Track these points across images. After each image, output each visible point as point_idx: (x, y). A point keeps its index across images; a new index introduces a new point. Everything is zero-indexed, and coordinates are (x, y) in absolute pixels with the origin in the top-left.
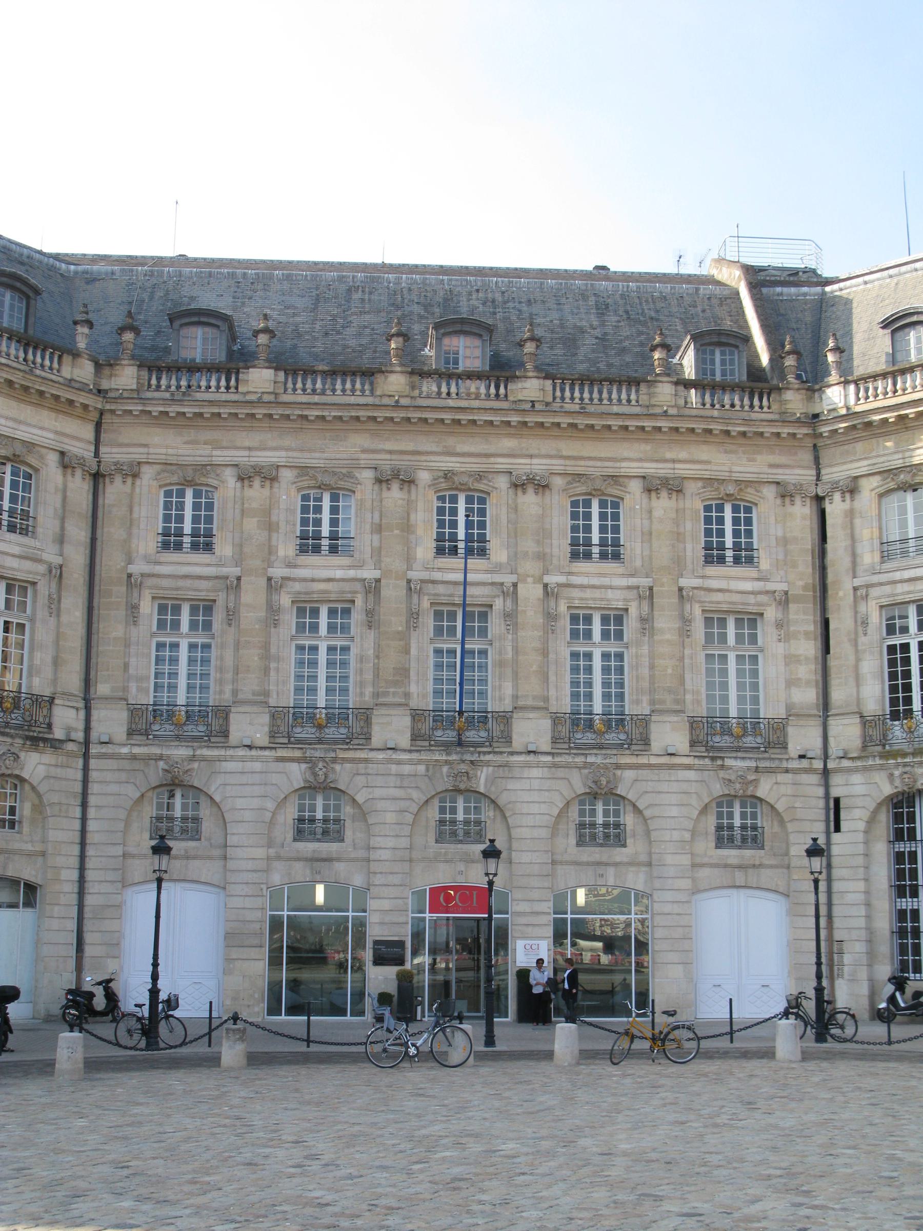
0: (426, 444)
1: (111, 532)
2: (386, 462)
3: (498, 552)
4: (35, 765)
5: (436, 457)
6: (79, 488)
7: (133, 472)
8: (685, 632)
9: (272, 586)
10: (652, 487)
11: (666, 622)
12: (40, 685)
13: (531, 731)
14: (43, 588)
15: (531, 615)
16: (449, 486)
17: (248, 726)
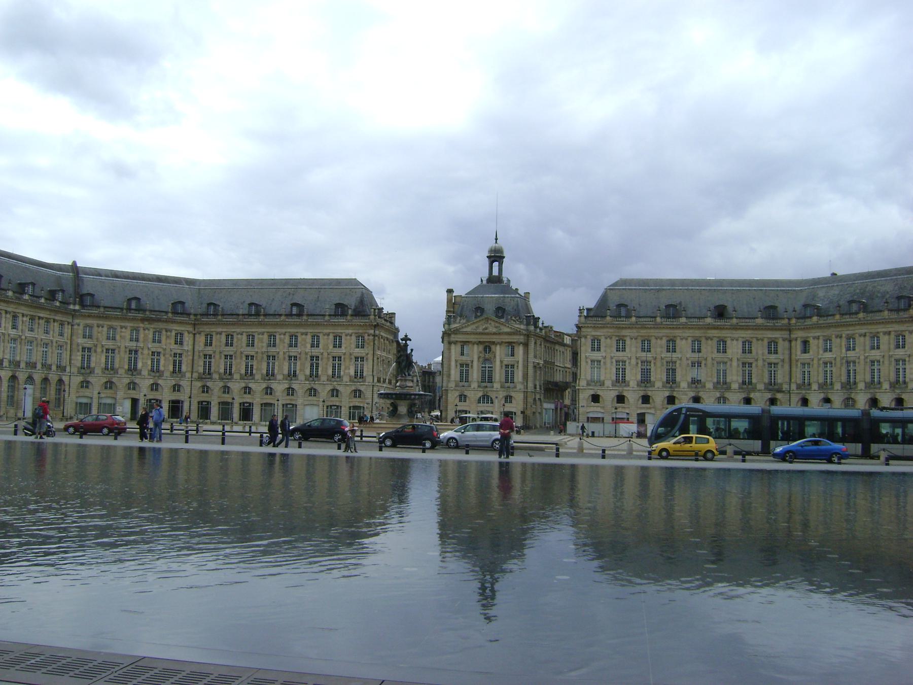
0: (844, 329)
1: (793, 351)
2: (837, 333)
3: (857, 350)
4: (779, 396)
5: (845, 332)
6: (787, 344)
7: (796, 340)
8: (890, 364)
9: (819, 359)
10: (885, 333)
11: (886, 362)
12: (779, 381)
13: (861, 386)
14: (780, 364)
15: (862, 362)
16: (849, 338)
17: (815, 386)
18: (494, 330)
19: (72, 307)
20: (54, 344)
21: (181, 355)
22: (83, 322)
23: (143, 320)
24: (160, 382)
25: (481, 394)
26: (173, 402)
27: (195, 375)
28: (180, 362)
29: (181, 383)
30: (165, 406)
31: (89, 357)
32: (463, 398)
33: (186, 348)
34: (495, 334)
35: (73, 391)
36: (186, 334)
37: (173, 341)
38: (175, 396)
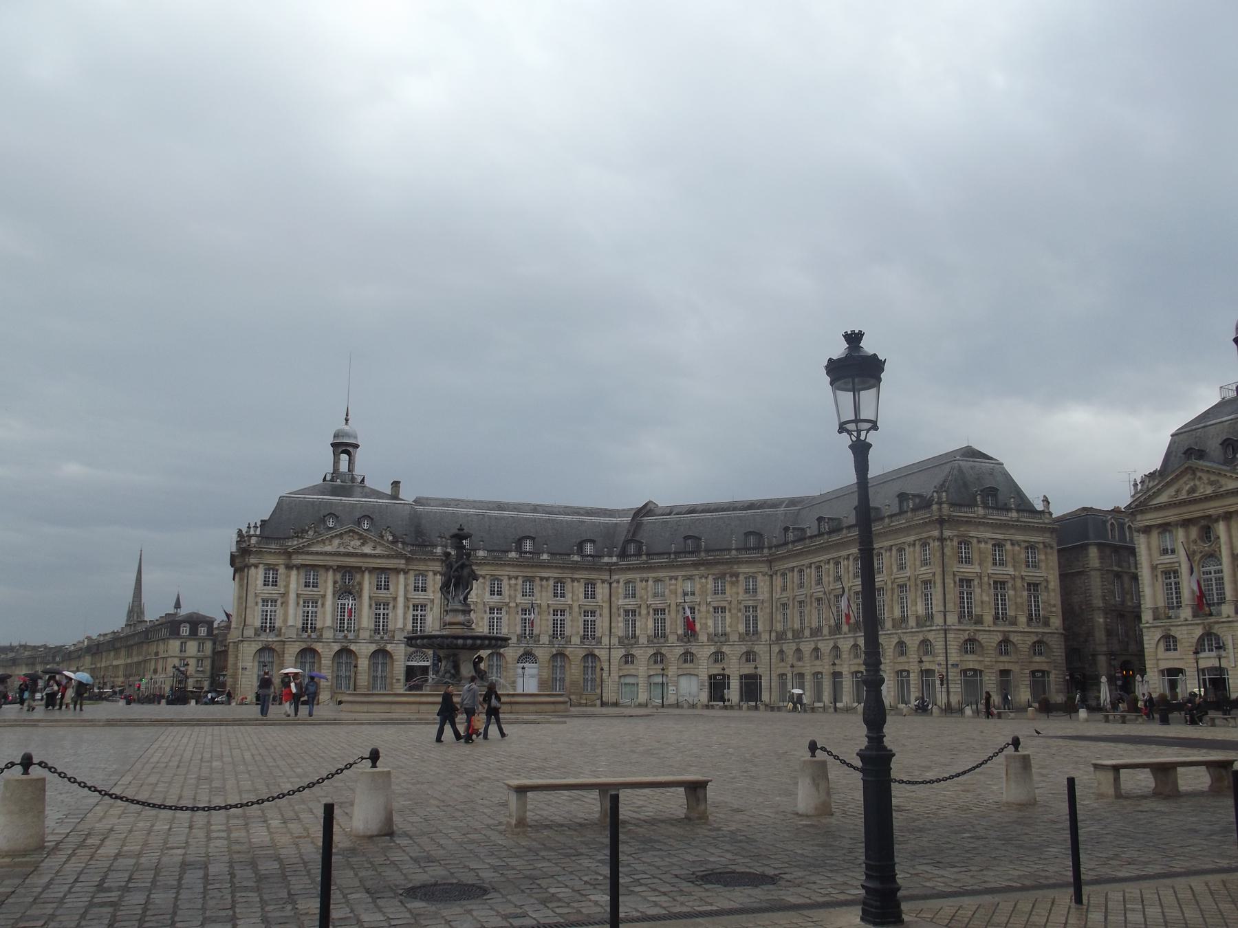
18: (1209, 490)
19: (606, 560)
20: (576, 609)
21: (755, 608)
22: (623, 578)
23: (696, 565)
24: (725, 649)
25: (1198, 632)
26: (747, 676)
27: (773, 635)
28: (755, 619)
29: (756, 649)
30: (735, 684)
31: (634, 622)
32: (1170, 641)
33: (761, 598)
34: (1208, 498)
35: (614, 668)
36: (760, 577)
37: (741, 590)
38: (748, 669)
